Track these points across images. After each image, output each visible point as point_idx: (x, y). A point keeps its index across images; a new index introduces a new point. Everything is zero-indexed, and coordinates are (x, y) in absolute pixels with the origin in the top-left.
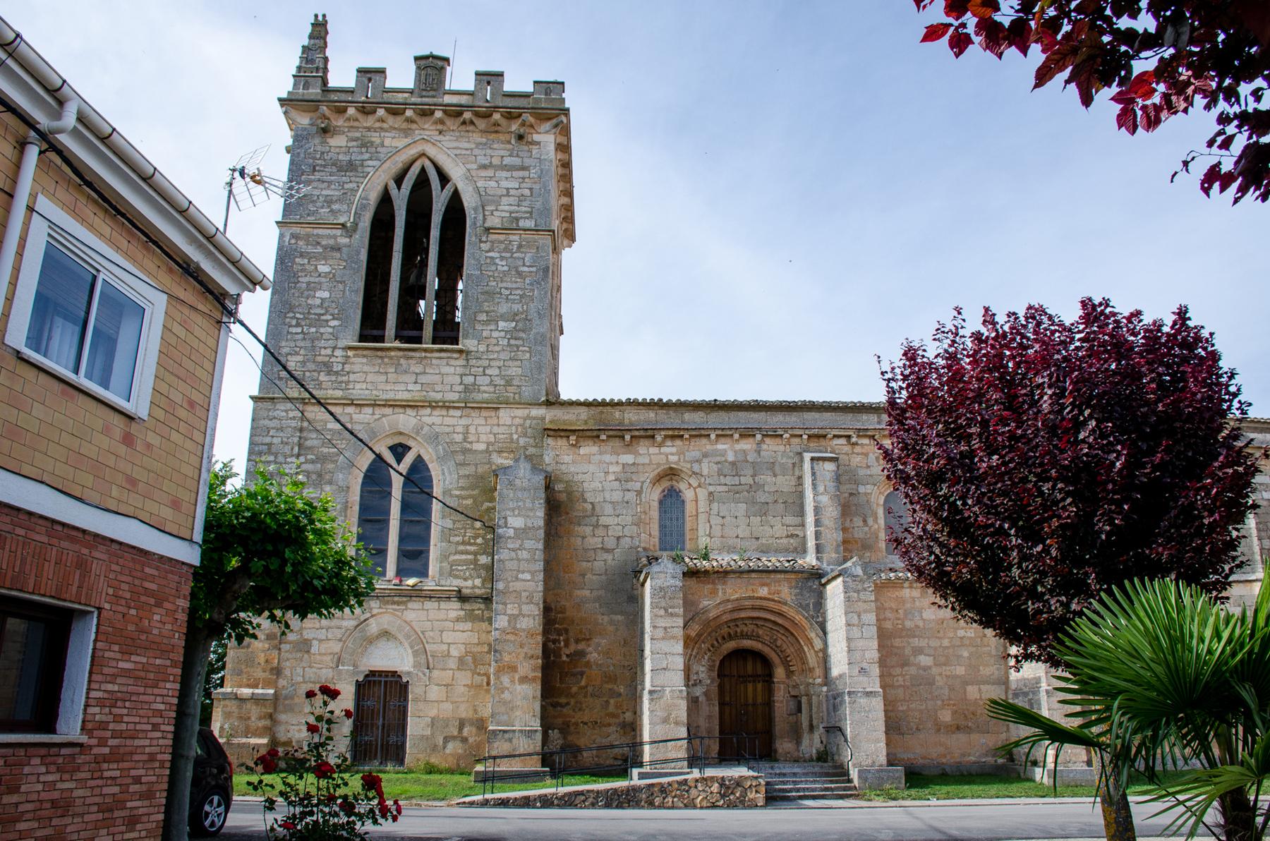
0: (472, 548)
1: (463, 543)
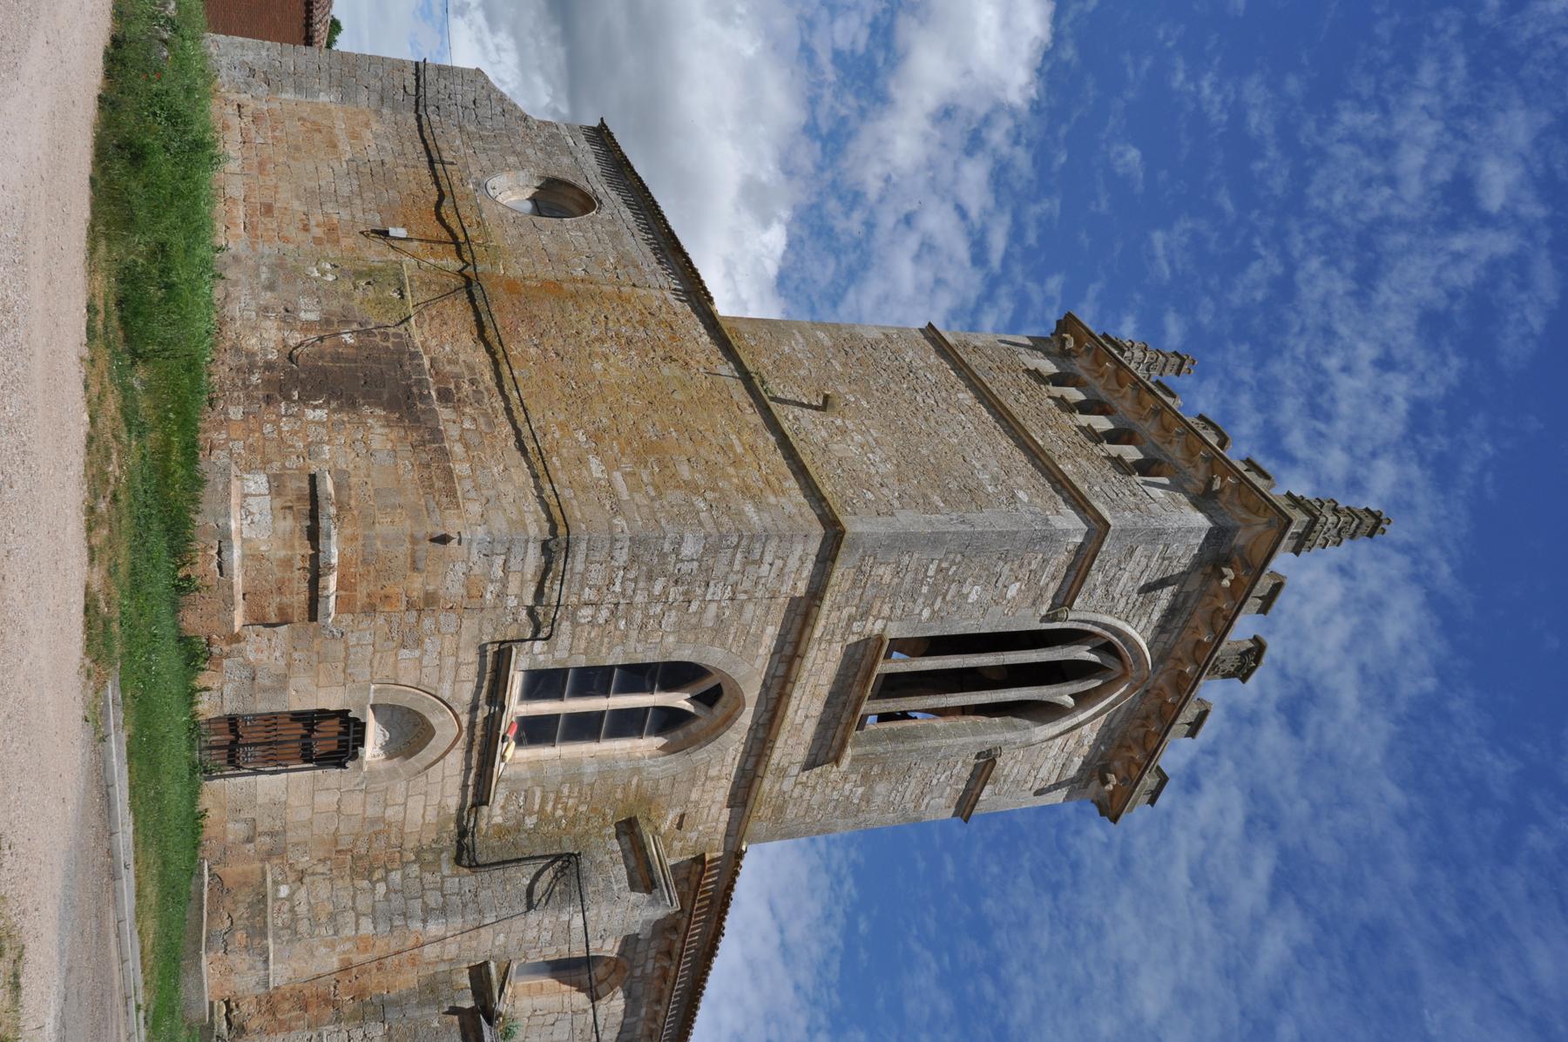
0: (549, 808)
1: (557, 800)
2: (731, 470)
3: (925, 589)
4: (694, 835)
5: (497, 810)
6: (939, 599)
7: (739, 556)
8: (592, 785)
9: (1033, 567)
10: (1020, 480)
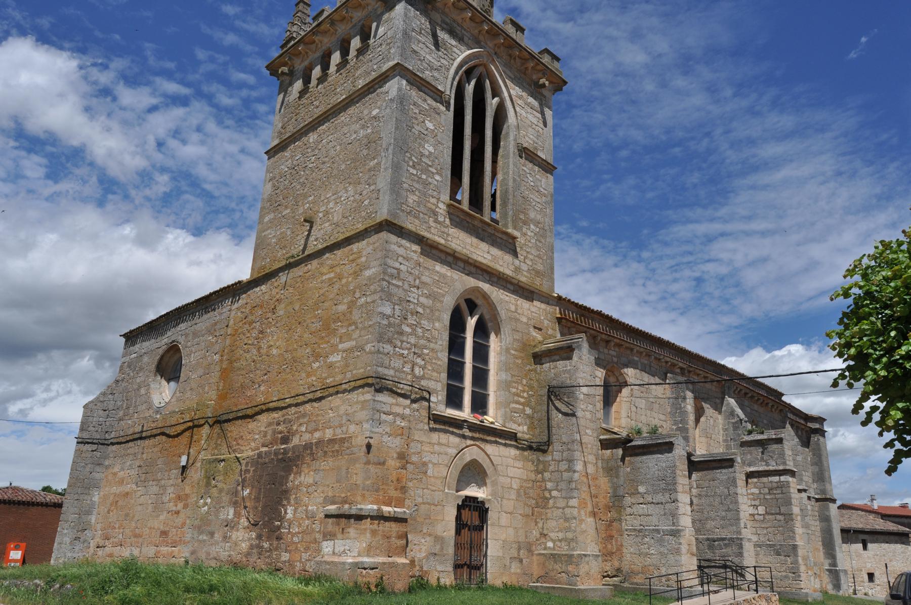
0: (522, 400)
1: (518, 395)
2: (344, 281)
3: (424, 177)
4: (546, 322)
5: (520, 429)
6: (430, 169)
7: (394, 282)
8: (513, 376)
9: (417, 111)
10: (366, 112)
